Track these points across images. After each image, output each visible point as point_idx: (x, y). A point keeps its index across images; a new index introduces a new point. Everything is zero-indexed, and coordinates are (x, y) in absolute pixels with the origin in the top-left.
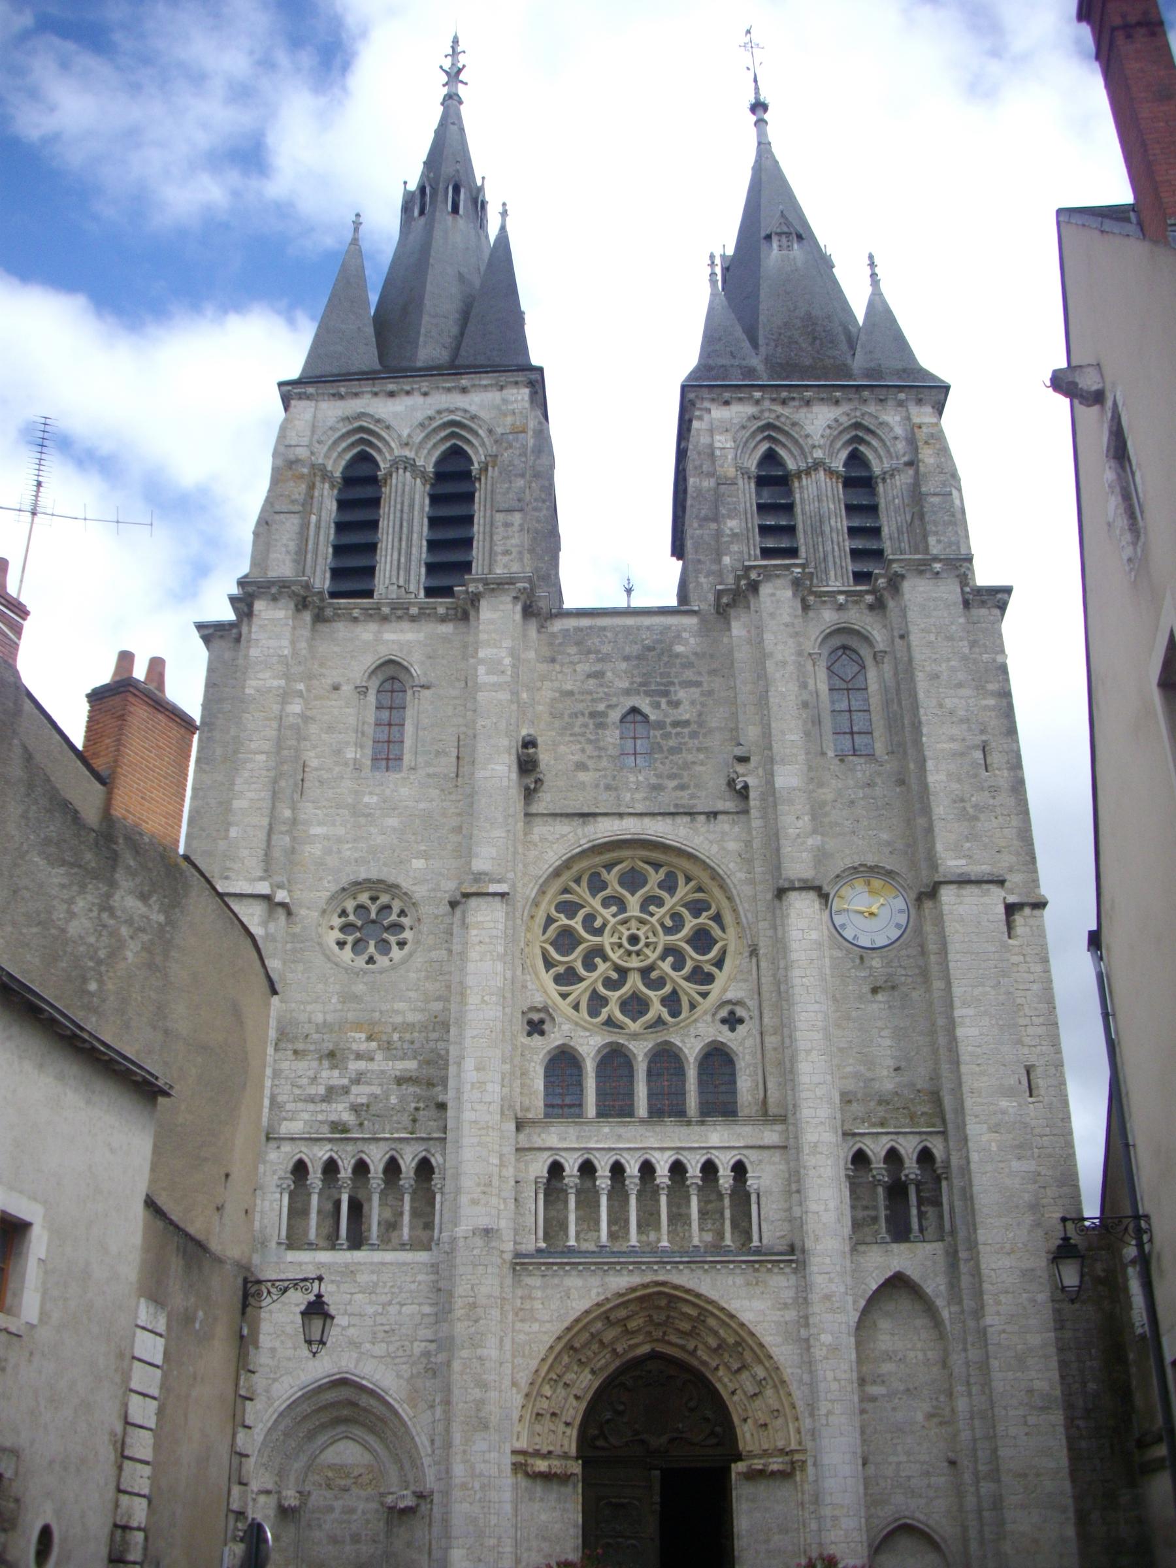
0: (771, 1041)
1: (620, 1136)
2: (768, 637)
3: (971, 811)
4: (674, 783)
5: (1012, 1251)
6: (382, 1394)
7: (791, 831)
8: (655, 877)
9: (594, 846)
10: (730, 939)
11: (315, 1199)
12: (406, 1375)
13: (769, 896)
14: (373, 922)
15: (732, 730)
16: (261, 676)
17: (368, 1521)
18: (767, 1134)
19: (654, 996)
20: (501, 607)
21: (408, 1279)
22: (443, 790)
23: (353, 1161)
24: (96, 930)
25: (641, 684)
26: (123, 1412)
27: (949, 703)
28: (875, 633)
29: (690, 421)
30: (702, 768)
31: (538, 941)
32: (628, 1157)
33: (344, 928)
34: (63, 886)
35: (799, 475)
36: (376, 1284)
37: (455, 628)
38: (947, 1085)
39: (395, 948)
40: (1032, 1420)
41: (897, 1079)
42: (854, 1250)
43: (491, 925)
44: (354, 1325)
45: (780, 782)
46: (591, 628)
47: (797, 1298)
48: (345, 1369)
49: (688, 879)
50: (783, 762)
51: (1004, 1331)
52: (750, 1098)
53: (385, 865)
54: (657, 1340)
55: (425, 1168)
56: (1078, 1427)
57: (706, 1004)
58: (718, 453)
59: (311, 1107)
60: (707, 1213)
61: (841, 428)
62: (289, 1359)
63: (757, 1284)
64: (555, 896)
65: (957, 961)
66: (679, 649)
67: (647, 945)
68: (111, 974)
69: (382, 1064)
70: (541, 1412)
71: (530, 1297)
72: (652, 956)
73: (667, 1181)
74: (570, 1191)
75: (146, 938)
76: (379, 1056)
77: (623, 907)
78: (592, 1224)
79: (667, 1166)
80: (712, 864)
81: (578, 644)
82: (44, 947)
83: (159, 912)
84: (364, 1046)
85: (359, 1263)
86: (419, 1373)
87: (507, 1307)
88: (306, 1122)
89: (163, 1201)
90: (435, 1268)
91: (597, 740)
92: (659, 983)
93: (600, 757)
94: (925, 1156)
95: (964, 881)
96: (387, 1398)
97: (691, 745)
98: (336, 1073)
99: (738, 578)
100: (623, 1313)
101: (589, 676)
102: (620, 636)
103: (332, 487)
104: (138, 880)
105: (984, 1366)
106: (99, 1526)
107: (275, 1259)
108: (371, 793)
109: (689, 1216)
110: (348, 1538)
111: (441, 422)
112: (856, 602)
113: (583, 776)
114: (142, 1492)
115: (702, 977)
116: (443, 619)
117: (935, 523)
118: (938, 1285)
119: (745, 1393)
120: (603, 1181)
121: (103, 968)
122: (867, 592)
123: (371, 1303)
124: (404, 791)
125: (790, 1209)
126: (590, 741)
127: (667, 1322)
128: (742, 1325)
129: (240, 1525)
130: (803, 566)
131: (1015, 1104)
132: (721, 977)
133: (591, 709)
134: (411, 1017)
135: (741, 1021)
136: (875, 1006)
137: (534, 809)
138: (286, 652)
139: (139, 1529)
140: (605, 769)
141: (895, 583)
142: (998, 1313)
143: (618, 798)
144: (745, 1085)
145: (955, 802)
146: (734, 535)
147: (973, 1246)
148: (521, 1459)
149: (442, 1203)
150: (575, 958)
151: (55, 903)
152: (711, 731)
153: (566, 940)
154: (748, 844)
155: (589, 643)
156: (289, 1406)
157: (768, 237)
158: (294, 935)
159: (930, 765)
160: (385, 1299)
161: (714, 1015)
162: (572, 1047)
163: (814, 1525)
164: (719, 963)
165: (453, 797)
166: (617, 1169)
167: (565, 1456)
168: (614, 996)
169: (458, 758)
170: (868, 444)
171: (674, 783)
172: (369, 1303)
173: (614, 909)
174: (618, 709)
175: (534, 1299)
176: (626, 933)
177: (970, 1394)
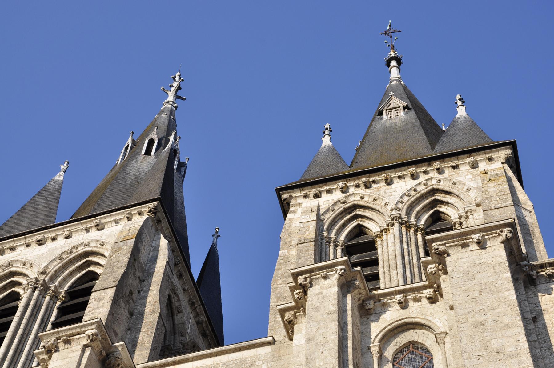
27: (495, 344)
35: (380, 236)
170: (447, 203)
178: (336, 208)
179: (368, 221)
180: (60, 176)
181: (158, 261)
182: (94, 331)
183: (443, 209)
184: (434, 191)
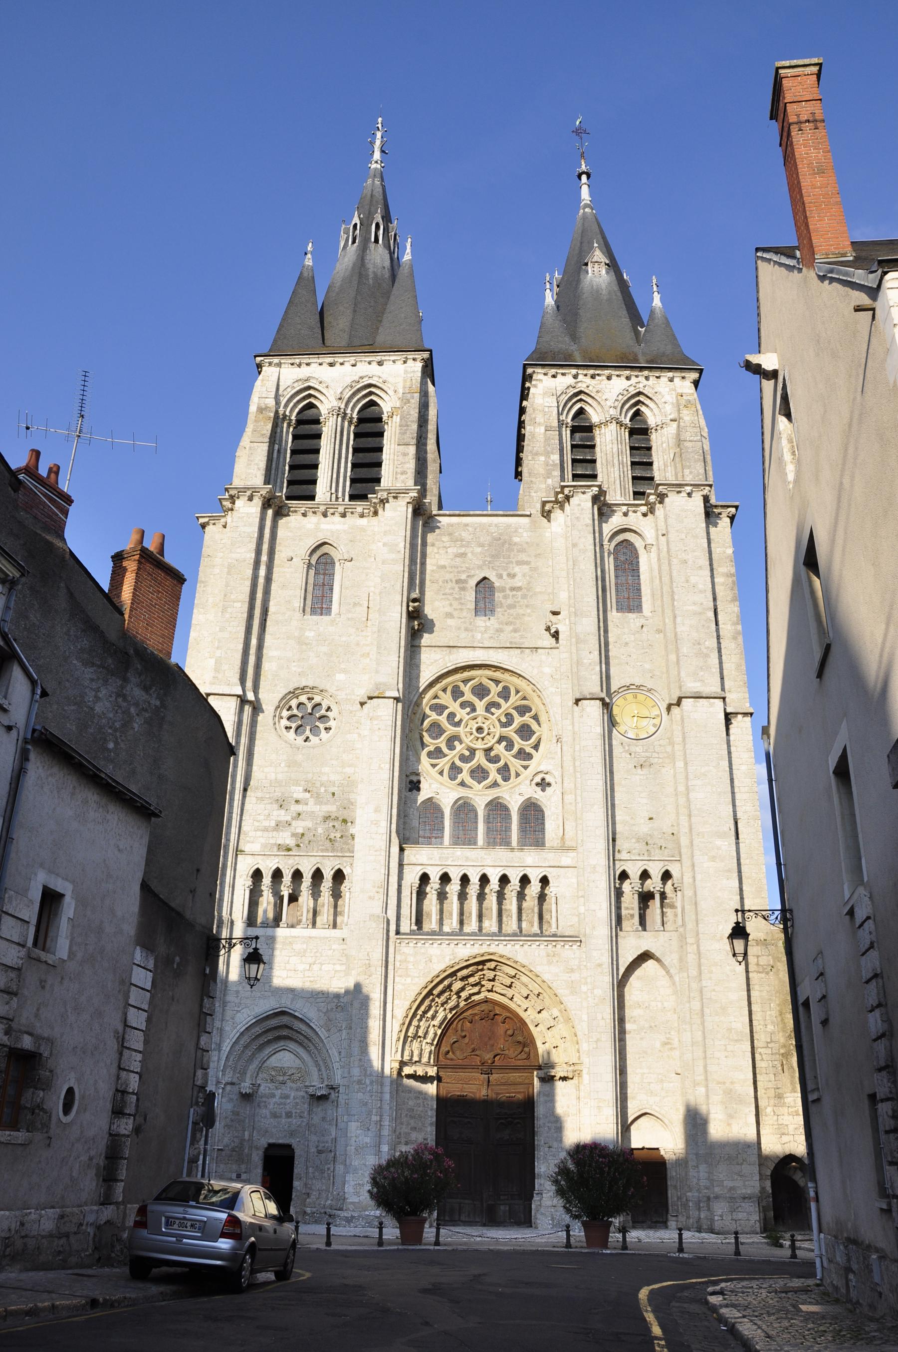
0: (569, 798)
1: (467, 859)
4: (511, 628)
6: (308, 1021)
7: (585, 661)
9: (457, 668)
10: (541, 731)
12: (325, 1010)
13: (571, 702)
14: (310, 714)
16: (238, 550)
17: (297, 1104)
19: (492, 768)
20: (399, 509)
22: (358, 629)
23: (292, 870)
24: (114, 709)
25: (490, 562)
26: (123, 1018)
27: (693, 580)
29: (529, 388)
30: (530, 619)
32: (473, 872)
34: (92, 680)
35: (599, 426)
36: (305, 951)
41: (650, 825)
43: (387, 718)
46: (458, 524)
48: (283, 1005)
49: (517, 692)
52: (554, 835)
54: (489, 991)
55: (339, 876)
57: (526, 774)
59: (266, 834)
61: (629, 395)
62: (247, 998)
66: (516, 539)
67: (489, 734)
68: (123, 738)
69: (311, 806)
75: (147, 715)
76: (311, 802)
77: (474, 710)
79: (498, 878)
81: (450, 534)
82: (79, 719)
83: (156, 698)
85: (295, 937)
89: (154, 885)
91: (461, 598)
93: (461, 609)
96: (311, 1024)
97: (521, 603)
98: (282, 812)
99: (557, 493)
100: (465, 972)
101: (456, 556)
102: (477, 530)
104: (143, 677)
106: (105, 1090)
108: (310, 630)
110: (284, 1114)
111: (363, 384)
112: (635, 512)
113: (450, 622)
114: (136, 1071)
115: (523, 755)
118: (672, 960)
121: (118, 734)
122: (642, 505)
126: (456, 599)
127: (493, 980)
128: (544, 982)
129: (201, 1095)
130: (600, 487)
133: (457, 578)
134: (333, 777)
135: (549, 784)
136: (637, 777)
139: (133, 1093)
141: (662, 497)
142: (710, 979)
143: (473, 636)
145: (694, 645)
151: (87, 690)
155: (457, 534)
156: (247, 1028)
157: (586, 264)
159: (679, 620)
160: (311, 960)
161: (532, 780)
164: (536, 747)
166: (465, 880)
168: (466, 767)
171: (511, 628)
173: (468, 710)
174: (475, 577)
176: (476, 725)
178: (568, 391)
179: (588, 406)
180: (309, 261)
181: (430, 408)
182: (416, 495)
183: (643, 409)
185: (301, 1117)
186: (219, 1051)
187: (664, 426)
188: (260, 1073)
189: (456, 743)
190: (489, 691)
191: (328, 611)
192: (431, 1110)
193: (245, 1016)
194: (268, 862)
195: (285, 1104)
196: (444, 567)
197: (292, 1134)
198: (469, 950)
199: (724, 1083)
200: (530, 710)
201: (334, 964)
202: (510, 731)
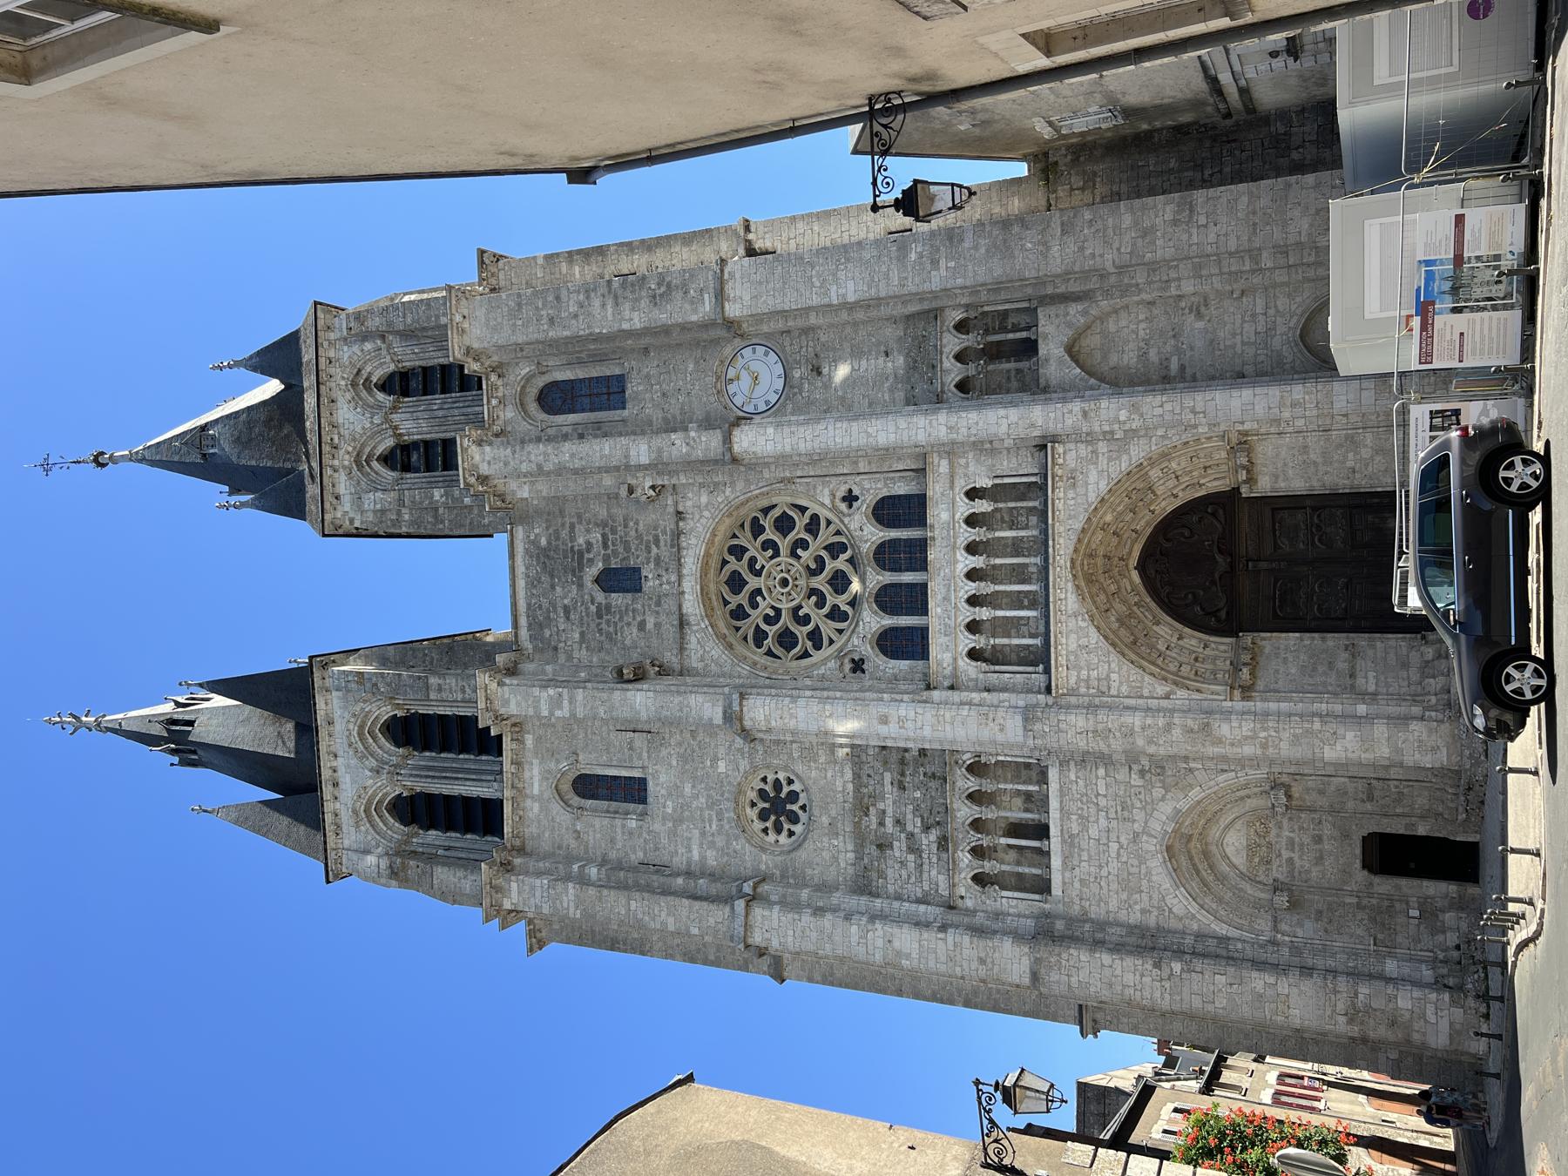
0: (863, 466)
2: (524, 468)
3: (663, 289)
5: (1045, 244)
7: (684, 451)
8: (733, 564)
10: (783, 501)
11: (1005, 868)
15: (609, 498)
16: (565, 905)
17: (1301, 828)
18: (941, 470)
19: (831, 566)
20: (507, 696)
21: (1074, 787)
22: (661, 745)
25: (574, 575)
28: (523, 372)
29: (357, 529)
30: (641, 525)
31: (789, 663)
33: (779, 830)
36: (1081, 817)
37: (529, 733)
38: (900, 310)
39: (793, 787)
40: (1202, 220)
41: (895, 353)
42: (1046, 390)
44: (1118, 837)
45: (644, 460)
47: (1086, 441)
49: (734, 536)
50: (627, 457)
51: (1118, 249)
53: (722, 795)
55: (976, 769)
56: (1211, 175)
58: (378, 507)
59: (926, 867)
60: (1013, 521)
63: (1074, 478)
64: (749, 649)
65: (790, 302)
66: (543, 542)
69: (888, 804)
70: (1193, 672)
71: (1087, 680)
72: (797, 567)
73: (981, 558)
74: (992, 642)
76: (881, 806)
77: (758, 592)
78: (1022, 622)
80: (719, 516)
81: (541, 626)
84: (874, 820)
85: (1062, 830)
86: (1160, 781)
87: (1097, 701)
88: (939, 873)
90: (1064, 764)
92: (820, 561)
94: (961, 327)
95: (720, 296)
98: (896, 844)
100: (1103, 596)
101: (568, 618)
102: (535, 592)
103: (417, 835)
105: (1153, 267)
107: (1061, 906)
109: (1014, 538)
110: (1317, 847)
113: (650, 625)
115: (813, 526)
116: (519, 741)
117: (429, 318)
119: (1176, 487)
120: (984, 613)
123: (1097, 821)
124: (663, 778)
125: (1008, 450)
126: (621, 619)
131: (913, 246)
132: (814, 508)
133: (595, 617)
134: (849, 775)
135: (850, 491)
137: (677, 667)
138: (546, 882)
140: (643, 606)
142: (1102, 256)
143: (666, 595)
144: (901, 489)
146: (446, 494)
147: (1040, 282)
148: (1237, 693)
149: (1006, 755)
150: (801, 632)
152: (610, 516)
153: (786, 639)
154: (702, 485)
158: (783, 876)
159: (625, 326)
160: (1093, 810)
162: (873, 636)
163: (1300, 423)
164: (803, 509)
165: (667, 736)
166: (973, 601)
167: (1237, 649)
168: (831, 600)
169: (634, 731)
172: (1098, 823)
173: (759, 599)
174: (594, 594)
175: (1089, 676)
177: (1179, 279)
182: (487, 675)
184: (354, 384)
185: (1320, 822)
186: (1229, 939)
187: (392, 351)
188: (1258, 879)
189: (801, 613)
190: (735, 571)
191: (642, 783)
192: (1302, 640)
193: (1175, 901)
194: (962, 865)
195: (1302, 845)
196: (582, 634)
197: (1346, 836)
198: (1069, 595)
199: (1255, 224)
200: (755, 519)
201: (1097, 777)
202: (784, 544)
